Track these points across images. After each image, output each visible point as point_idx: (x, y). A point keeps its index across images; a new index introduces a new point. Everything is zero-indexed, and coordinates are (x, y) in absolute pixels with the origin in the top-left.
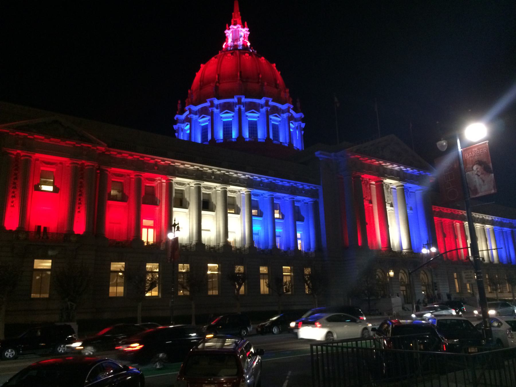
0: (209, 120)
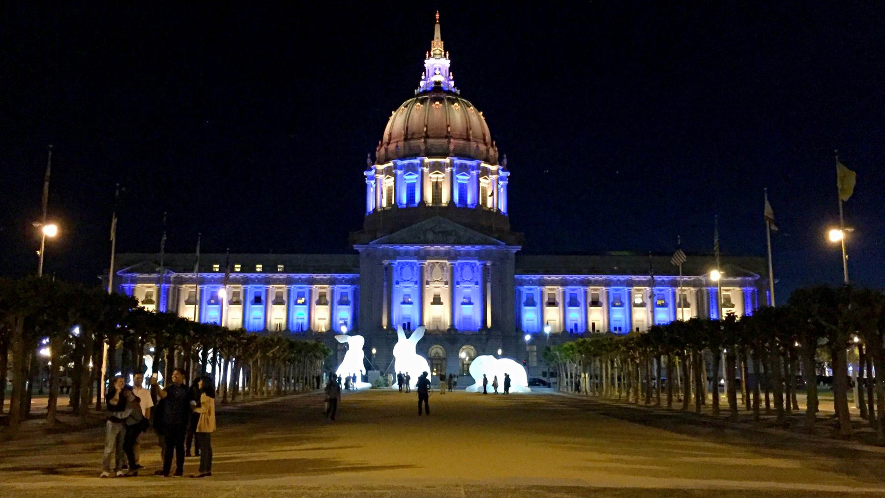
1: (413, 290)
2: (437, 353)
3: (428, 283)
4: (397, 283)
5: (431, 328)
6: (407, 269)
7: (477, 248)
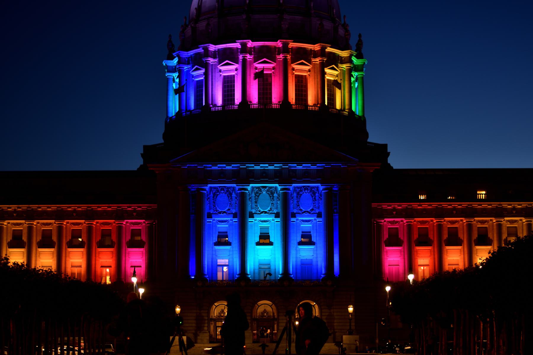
0: (236, 69)
1: (230, 225)
2: (265, 311)
3: (252, 215)
4: (210, 216)
5: (257, 278)
6: (222, 197)
7: (319, 166)
